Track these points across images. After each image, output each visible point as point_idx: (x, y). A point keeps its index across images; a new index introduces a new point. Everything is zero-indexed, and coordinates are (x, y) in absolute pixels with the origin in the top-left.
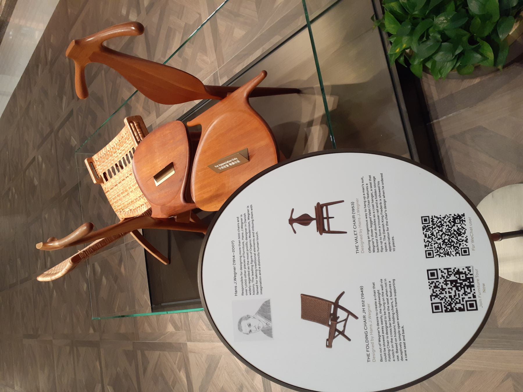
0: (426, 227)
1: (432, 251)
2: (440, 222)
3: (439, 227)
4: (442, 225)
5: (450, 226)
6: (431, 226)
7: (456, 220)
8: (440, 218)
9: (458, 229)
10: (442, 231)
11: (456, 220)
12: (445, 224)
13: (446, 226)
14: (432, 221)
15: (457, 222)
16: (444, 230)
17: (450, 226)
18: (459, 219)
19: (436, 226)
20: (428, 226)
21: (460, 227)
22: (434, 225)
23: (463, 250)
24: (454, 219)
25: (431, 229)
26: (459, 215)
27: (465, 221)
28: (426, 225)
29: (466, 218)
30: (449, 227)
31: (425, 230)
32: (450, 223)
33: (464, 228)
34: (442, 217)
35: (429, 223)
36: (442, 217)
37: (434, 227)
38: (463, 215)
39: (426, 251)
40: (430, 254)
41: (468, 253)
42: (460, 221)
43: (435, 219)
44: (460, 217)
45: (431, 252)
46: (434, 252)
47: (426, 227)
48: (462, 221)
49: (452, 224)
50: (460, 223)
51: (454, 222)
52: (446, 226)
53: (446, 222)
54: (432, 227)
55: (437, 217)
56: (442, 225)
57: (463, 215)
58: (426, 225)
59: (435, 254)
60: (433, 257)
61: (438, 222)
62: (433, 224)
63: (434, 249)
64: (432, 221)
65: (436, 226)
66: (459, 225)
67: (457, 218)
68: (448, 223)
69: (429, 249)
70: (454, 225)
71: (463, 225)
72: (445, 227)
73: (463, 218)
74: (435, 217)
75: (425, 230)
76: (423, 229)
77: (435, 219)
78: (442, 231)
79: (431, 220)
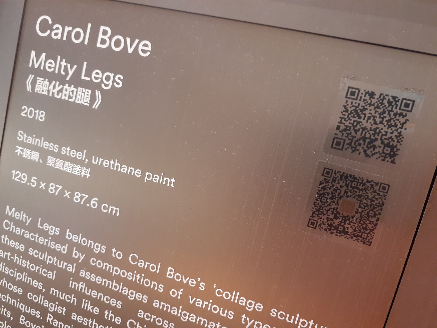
0: (396, 102)
1: (356, 99)
2: (396, 126)
3: (389, 121)
4: (390, 126)
5: (384, 137)
6: (394, 109)
7: (389, 149)
8: (402, 128)
9: (375, 147)
10: (381, 122)
11: (389, 149)
12: (389, 131)
13: (386, 132)
14: (401, 114)
15: (386, 148)
16: (381, 126)
17: (384, 137)
18: (389, 155)
19: (392, 116)
20: (397, 105)
21: (376, 150)
22: (395, 114)
23: (342, 141)
24: (392, 147)
25: (390, 108)
26: (395, 155)
27: (384, 160)
28: (399, 104)
29: (387, 164)
30: (383, 135)
31: (391, 100)
32: (388, 139)
33: (372, 156)
34: (403, 130)
35: (400, 109)
36: (403, 130)
37: (392, 113)
38: (393, 162)
39: (359, 90)
40: (353, 94)
41: (334, 146)
42: (386, 154)
43: (402, 120)
44: (391, 156)
45: (355, 97)
46: (354, 101)
47: (396, 102)
48: (385, 157)
49: (386, 142)
50: (383, 152)
51: (388, 145)
52: (386, 132)
53: (392, 133)
54: (392, 111)
55: (405, 123)
56: (390, 126)
57: (393, 162)
58: (399, 104)
59: (350, 101)
60: (346, 97)
61: (397, 122)
62: (395, 114)
63: (358, 102)
64: (401, 114)
65: (392, 116)
66: (381, 150)
67: (392, 150)
68: (389, 135)
69: (360, 95)
70: (382, 143)
71: (378, 155)
72: (385, 129)
73: (388, 159)
74: (407, 120)
75: (391, 100)
76: (394, 98)
77: (402, 120)
78: (381, 122)
79: (404, 113)
